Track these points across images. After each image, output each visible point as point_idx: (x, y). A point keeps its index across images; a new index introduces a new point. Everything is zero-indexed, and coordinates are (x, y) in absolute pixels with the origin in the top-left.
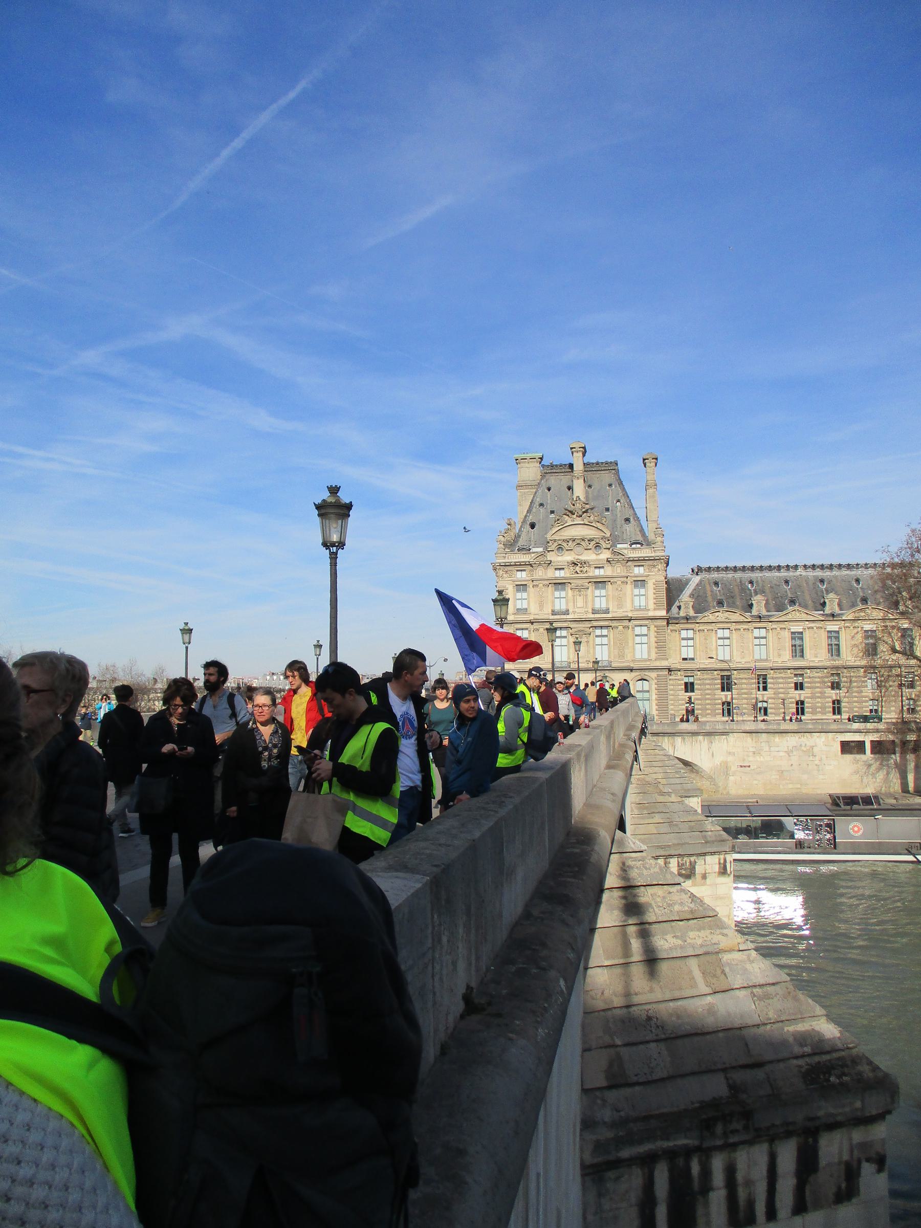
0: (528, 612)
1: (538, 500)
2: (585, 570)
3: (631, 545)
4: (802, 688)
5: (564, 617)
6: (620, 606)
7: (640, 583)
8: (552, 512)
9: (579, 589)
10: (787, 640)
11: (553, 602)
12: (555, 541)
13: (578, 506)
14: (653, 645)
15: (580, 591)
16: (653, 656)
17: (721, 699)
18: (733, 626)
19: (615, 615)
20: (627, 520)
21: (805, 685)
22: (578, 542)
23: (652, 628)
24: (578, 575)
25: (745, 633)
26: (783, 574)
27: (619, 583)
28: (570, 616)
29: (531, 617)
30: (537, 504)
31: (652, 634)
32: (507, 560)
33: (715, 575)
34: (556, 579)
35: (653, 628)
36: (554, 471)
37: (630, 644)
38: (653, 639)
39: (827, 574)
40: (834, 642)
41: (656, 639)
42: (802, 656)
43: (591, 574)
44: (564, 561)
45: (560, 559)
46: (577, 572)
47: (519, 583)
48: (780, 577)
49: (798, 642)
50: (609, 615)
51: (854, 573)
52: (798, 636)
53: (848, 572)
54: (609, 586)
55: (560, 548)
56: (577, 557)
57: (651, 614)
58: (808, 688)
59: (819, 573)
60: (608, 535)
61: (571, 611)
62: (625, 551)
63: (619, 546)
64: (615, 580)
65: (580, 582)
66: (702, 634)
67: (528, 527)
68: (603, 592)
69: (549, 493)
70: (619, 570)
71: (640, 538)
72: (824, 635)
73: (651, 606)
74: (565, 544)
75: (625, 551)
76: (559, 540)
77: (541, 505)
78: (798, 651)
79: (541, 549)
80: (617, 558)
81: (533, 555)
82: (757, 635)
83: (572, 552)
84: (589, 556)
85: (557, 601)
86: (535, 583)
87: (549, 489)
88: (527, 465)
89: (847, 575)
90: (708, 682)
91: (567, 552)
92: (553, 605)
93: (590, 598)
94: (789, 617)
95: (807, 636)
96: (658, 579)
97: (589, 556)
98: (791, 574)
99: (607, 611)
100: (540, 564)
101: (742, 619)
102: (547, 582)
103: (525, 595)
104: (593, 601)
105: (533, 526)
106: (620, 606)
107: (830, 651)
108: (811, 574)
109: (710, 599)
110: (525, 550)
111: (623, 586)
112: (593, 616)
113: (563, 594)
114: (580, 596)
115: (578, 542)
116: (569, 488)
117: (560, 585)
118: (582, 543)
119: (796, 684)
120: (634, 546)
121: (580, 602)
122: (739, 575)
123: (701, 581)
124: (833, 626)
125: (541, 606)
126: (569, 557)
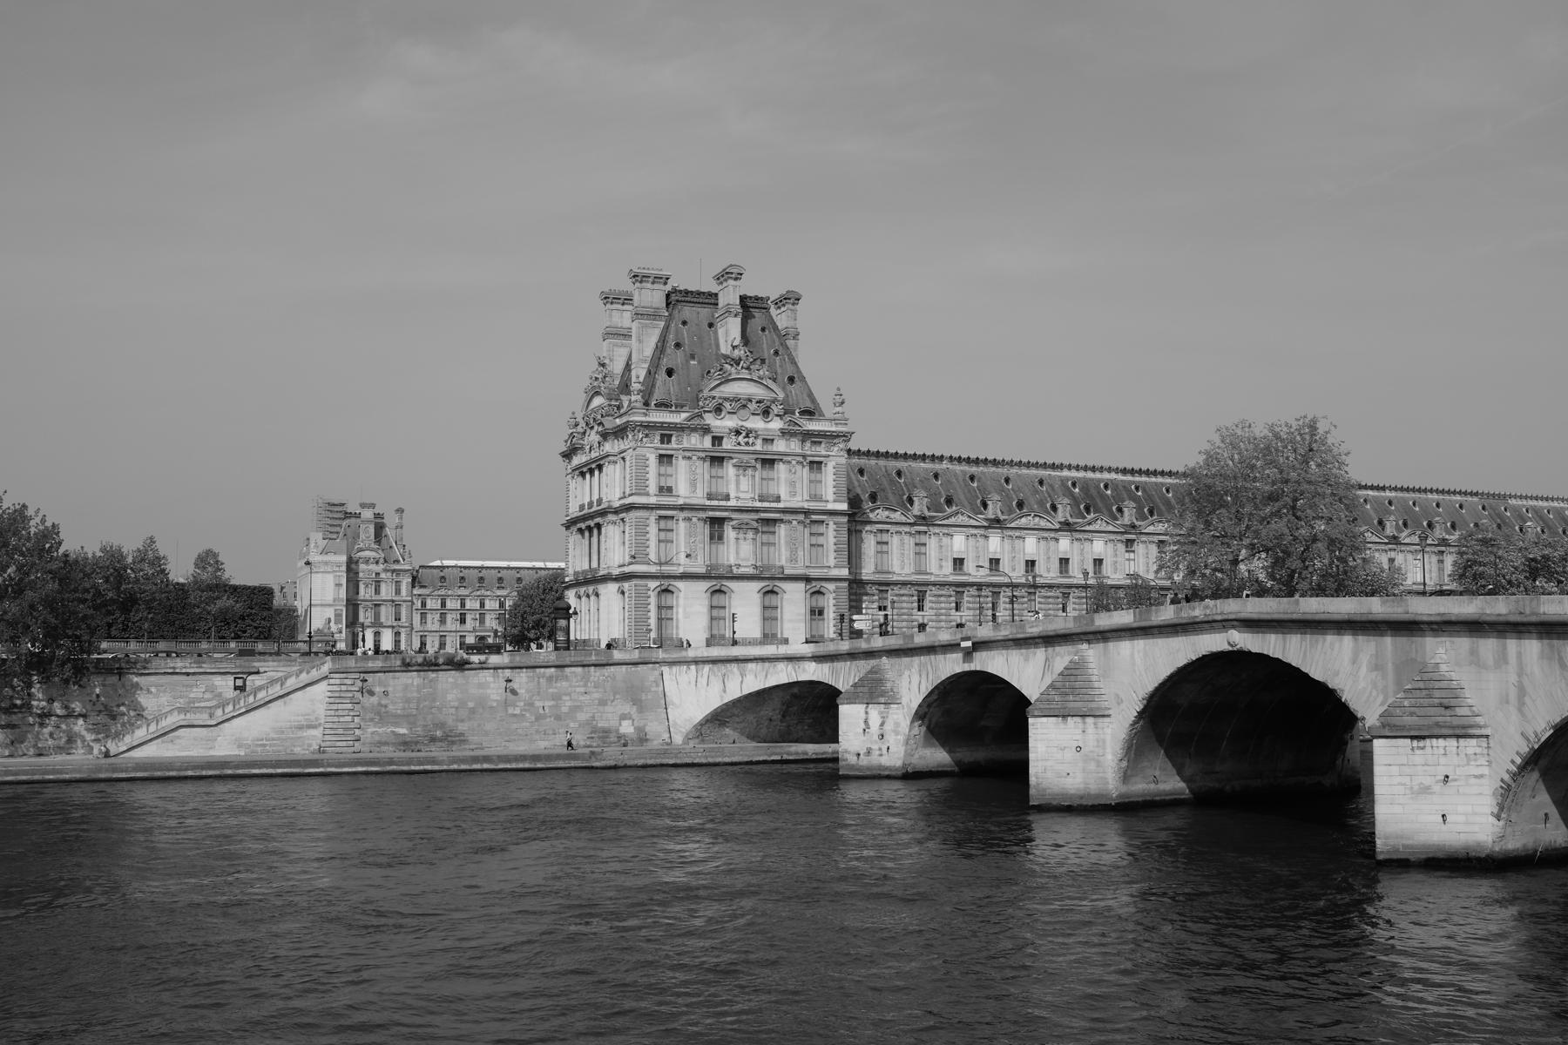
0: (674, 493)
2: (751, 441)
5: (723, 503)
6: (793, 494)
8: (693, 357)
9: (742, 467)
12: (714, 398)
14: (832, 547)
17: (879, 620)
18: (893, 528)
19: (788, 505)
22: (744, 402)
24: (742, 448)
25: (906, 538)
26: (928, 465)
27: (794, 462)
28: (732, 503)
29: (681, 501)
32: (648, 419)
35: (832, 526)
36: (688, 299)
38: (832, 540)
41: (834, 540)
45: (718, 423)
46: (739, 444)
48: (927, 470)
50: (781, 505)
51: (1004, 471)
53: (994, 469)
55: (718, 410)
56: (741, 423)
57: (831, 506)
60: (781, 396)
61: (732, 495)
64: (789, 458)
65: (745, 457)
67: (661, 376)
69: (685, 330)
70: (794, 446)
73: (830, 497)
76: (720, 398)
83: (735, 416)
84: (757, 423)
87: (684, 323)
88: (649, 285)
89: (994, 472)
91: (728, 416)
94: (952, 521)
96: (839, 462)
97: (757, 423)
98: (937, 466)
100: (694, 430)
101: (904, 519)
102: (703, 455)
105: (670, 373)
111: (799, 467)
112: (758, 504)
114: (744, 476)
115: (742, 404)
116: (711, 325)
121: (745, 484)
125: (693, 484)
126: (730, 422)
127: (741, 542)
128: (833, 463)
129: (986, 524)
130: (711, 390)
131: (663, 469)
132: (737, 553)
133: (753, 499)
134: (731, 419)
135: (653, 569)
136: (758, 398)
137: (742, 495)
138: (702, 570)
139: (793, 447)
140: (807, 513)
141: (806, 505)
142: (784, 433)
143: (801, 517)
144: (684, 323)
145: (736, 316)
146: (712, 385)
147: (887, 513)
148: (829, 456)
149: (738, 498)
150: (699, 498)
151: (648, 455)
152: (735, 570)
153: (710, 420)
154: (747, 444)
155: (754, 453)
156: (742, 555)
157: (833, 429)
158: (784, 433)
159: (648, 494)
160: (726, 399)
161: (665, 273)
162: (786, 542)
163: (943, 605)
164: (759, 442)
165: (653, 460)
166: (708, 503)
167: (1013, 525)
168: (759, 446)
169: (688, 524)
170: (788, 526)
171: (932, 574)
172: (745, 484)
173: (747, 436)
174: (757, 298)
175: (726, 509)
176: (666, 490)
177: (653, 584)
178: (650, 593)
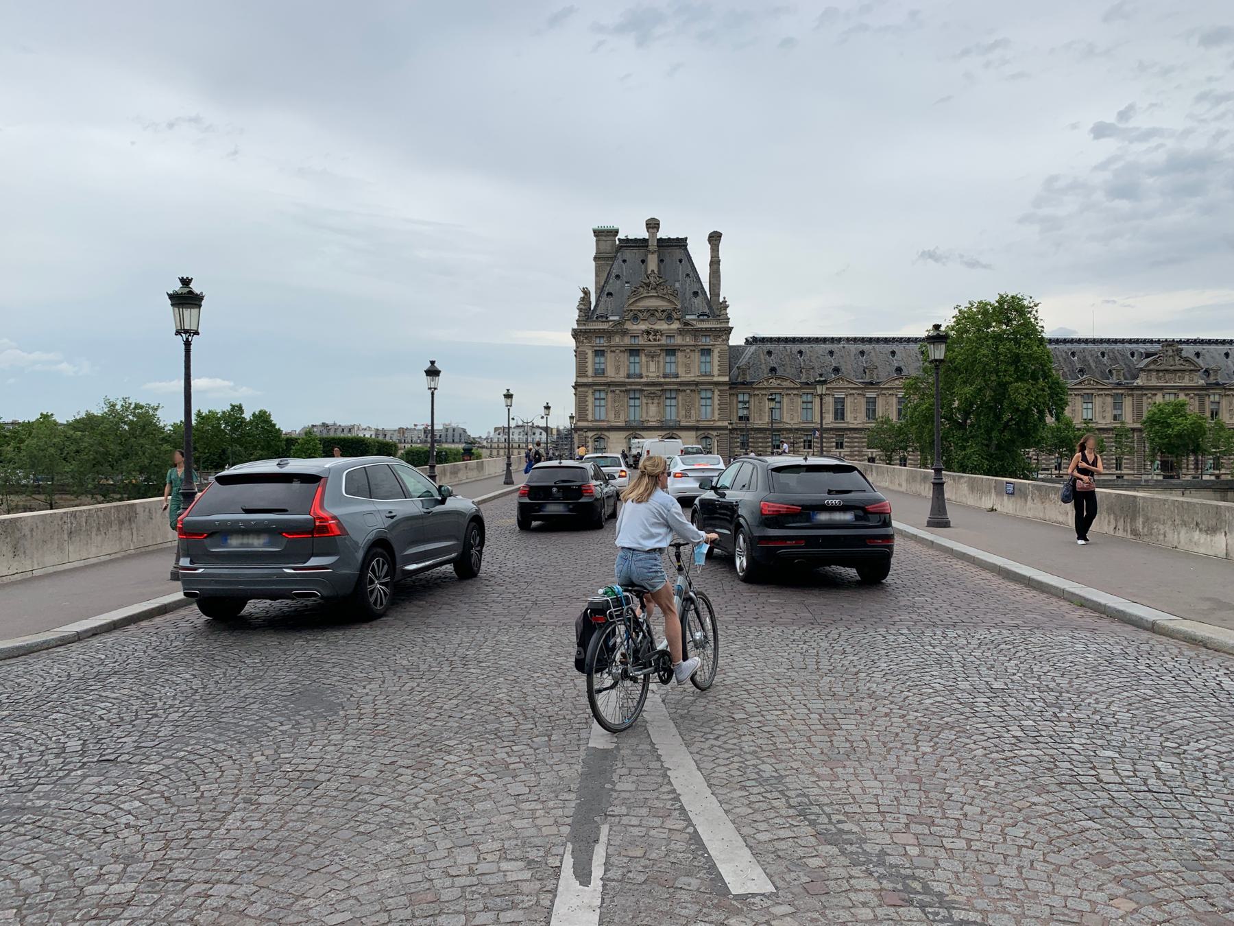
1: (615, 272)
3: (698, 316)
4: (842, 447)
6: (688, 372)
7: (706, 352)
9: (652, 356)
10: (831, 404)
11: (628, 366)
12: (631, 311)
13: (652, 280)
14: (716, 407)
15: (653, 357)
16: (716, 417)
18: (784, 392)
19: (683, 379)
20: (696, 294)
21: (845, 444)
23: (717, 393)
26: (829, 347)
29: (609, 380)
30: (613, 275)
31: (716, 397)
33: (768, 346)
34: (631, 345)
35: (717, 393)
37: (697, 406)
38: (716, 402)
39: (866, 347)
40: (871, 407)
42: (843, 419)
43: (663, 342)
44: (639, 330)
46: (650, 340)
47: (598, 348)
49: (871, 407)
50: (678, 380)
52: (840, 403)
54: (679, 354)
55: (635, 318)
56: (651, 326)
57: (715, 379)
58: (848, 447)
59: (862, 347)
61: (644, 375)
62: (694, 322)
63: (688, 317)
65: (653, 349)
66: (757, 398)
67: (604, 297)
68: (673, 359)
69: (624, 266)
70: (689, 340)
71: (707, 310)
72: (863, 401)
73: (716, 372)
74: (640, 315)
75: (694, 322)
77: (618, 277)
78: (840, 414)
79: (616, 318)
80: (686, 329)
81: (611, 323)
82: (805, 400)
85: (632, 365)
86: (613, 349)
87: (624, 261)
88: (604, 238)
90: (760, 440)
92: (629, 370)
93: (662, 364)
95: (848, 402)
97: (662, 326)
98: (834, 347)
99: (677, 376)
100: (616, 333)
101: (792, 385)
103: (602, 360)
104: (664, 366)
106: (688, 372)
107: (867, 416)
108: (854, 348)
109: (763, 367)
110: (604, 318)
111: (692, 354)
112: (663, 380)
113: (637, 359)
115: (652, 312)
116: (643, 261)
117: (634, 352)
118: (656, 314)
119: (837, 443)
120: (701, 318)
121: (653, 366)
122: (788, 346)
123: (756, 350)
124: (871, 394)
125: (618, 368)
127: (650, 405)
128: (718, 349)
129: (861, 386)
130: (630, 305)
131: (597, 360)
132: (647, 413)
133: (658, 377)
134: (644, 324)
135: (590, 424)
136: (662, 309)
137: (651, 375)
138: (623, 424)
139: (688, 340)
140: (697, 384)
141: (697, 379)
142: (681, 332)
143: (694, 388)
144: (624, 261)
145: (653, 253)
146: (630, 302)
147: (779, 382)
148: (715, 345)
149: (647, 376)
150: (621, 377)
151: (587, 351)
152: (646, 424)
153: (629, 326)
154: (655, 340)
155: (659, 345)
156: (651, 413)
157: (718, 326)
158: (681, 332)
159: (587, 376)
160: (640, 311)
161: (616, 227)
162: (683, 404)
163: (856, 444)
164: (664, 338)
165: (590, 354)
166: (627, 380)
167: (885, 386)
168: (663, 341)
169: (613, 395)
170: (683, 394)
171: (848, 423)
172: (653, 366)
173: (655, 335)
174: (678, 239)
175: (639, 384)
176: (600, 372)
177: (590, 434)
178: (589, 440)
